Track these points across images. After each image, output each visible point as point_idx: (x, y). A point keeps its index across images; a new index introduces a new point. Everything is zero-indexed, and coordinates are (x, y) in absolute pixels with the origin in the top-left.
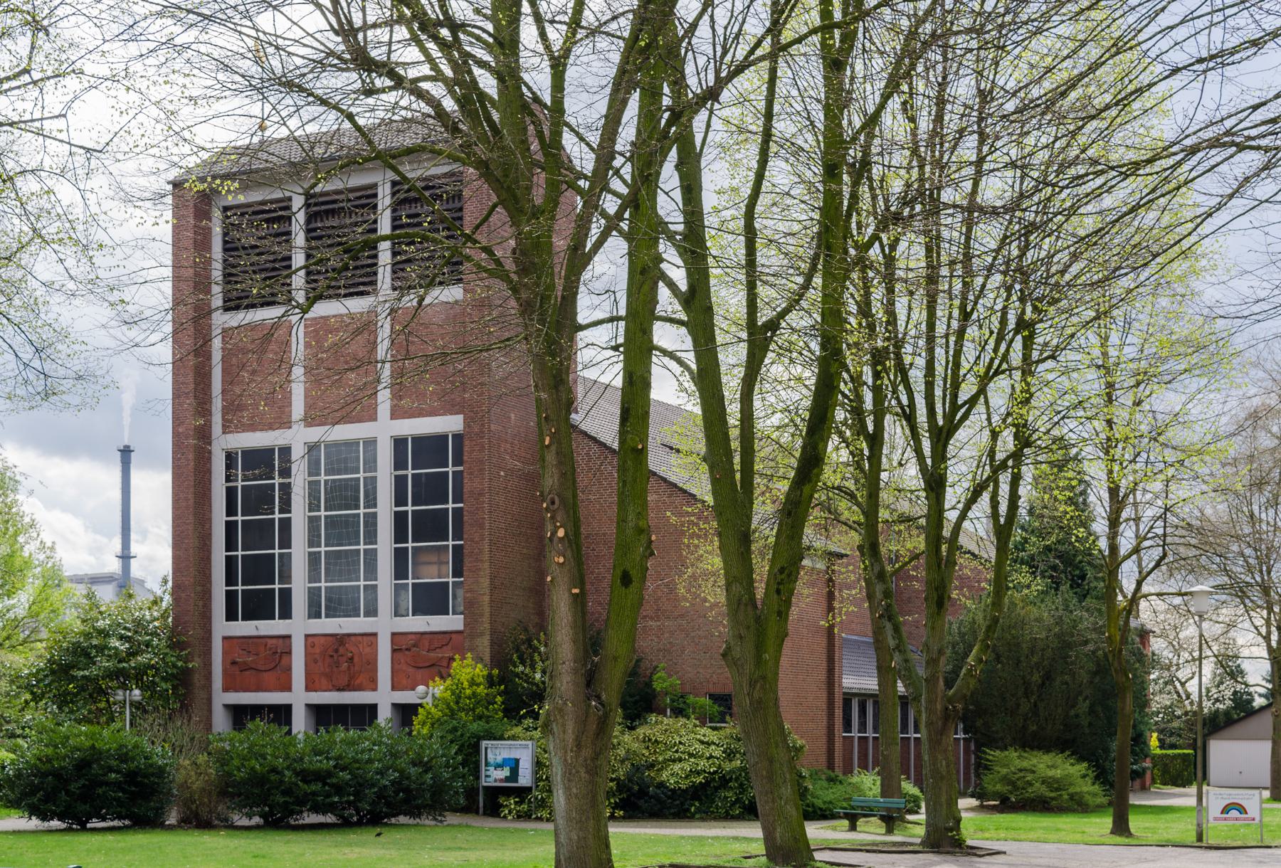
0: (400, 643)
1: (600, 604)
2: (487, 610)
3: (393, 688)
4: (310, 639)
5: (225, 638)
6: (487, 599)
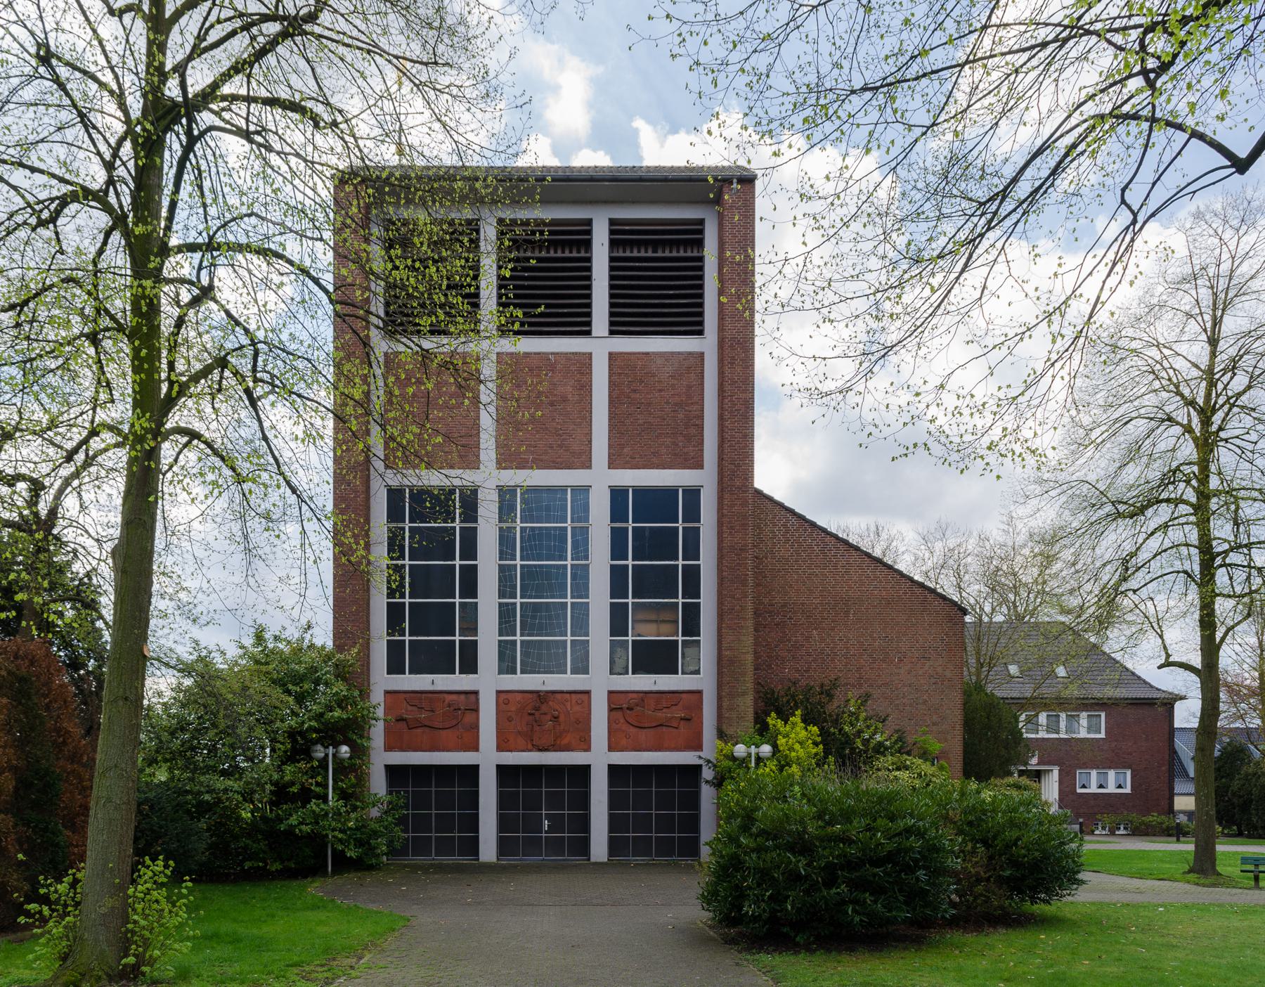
0: (617, 702)
1: (797, 671)
2: (750, 668)
3: (611, 749)
4: (503, 696)
5: (387, 692)
6: (750, 658)
